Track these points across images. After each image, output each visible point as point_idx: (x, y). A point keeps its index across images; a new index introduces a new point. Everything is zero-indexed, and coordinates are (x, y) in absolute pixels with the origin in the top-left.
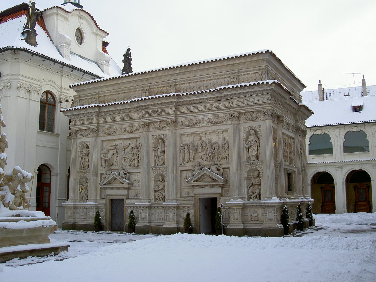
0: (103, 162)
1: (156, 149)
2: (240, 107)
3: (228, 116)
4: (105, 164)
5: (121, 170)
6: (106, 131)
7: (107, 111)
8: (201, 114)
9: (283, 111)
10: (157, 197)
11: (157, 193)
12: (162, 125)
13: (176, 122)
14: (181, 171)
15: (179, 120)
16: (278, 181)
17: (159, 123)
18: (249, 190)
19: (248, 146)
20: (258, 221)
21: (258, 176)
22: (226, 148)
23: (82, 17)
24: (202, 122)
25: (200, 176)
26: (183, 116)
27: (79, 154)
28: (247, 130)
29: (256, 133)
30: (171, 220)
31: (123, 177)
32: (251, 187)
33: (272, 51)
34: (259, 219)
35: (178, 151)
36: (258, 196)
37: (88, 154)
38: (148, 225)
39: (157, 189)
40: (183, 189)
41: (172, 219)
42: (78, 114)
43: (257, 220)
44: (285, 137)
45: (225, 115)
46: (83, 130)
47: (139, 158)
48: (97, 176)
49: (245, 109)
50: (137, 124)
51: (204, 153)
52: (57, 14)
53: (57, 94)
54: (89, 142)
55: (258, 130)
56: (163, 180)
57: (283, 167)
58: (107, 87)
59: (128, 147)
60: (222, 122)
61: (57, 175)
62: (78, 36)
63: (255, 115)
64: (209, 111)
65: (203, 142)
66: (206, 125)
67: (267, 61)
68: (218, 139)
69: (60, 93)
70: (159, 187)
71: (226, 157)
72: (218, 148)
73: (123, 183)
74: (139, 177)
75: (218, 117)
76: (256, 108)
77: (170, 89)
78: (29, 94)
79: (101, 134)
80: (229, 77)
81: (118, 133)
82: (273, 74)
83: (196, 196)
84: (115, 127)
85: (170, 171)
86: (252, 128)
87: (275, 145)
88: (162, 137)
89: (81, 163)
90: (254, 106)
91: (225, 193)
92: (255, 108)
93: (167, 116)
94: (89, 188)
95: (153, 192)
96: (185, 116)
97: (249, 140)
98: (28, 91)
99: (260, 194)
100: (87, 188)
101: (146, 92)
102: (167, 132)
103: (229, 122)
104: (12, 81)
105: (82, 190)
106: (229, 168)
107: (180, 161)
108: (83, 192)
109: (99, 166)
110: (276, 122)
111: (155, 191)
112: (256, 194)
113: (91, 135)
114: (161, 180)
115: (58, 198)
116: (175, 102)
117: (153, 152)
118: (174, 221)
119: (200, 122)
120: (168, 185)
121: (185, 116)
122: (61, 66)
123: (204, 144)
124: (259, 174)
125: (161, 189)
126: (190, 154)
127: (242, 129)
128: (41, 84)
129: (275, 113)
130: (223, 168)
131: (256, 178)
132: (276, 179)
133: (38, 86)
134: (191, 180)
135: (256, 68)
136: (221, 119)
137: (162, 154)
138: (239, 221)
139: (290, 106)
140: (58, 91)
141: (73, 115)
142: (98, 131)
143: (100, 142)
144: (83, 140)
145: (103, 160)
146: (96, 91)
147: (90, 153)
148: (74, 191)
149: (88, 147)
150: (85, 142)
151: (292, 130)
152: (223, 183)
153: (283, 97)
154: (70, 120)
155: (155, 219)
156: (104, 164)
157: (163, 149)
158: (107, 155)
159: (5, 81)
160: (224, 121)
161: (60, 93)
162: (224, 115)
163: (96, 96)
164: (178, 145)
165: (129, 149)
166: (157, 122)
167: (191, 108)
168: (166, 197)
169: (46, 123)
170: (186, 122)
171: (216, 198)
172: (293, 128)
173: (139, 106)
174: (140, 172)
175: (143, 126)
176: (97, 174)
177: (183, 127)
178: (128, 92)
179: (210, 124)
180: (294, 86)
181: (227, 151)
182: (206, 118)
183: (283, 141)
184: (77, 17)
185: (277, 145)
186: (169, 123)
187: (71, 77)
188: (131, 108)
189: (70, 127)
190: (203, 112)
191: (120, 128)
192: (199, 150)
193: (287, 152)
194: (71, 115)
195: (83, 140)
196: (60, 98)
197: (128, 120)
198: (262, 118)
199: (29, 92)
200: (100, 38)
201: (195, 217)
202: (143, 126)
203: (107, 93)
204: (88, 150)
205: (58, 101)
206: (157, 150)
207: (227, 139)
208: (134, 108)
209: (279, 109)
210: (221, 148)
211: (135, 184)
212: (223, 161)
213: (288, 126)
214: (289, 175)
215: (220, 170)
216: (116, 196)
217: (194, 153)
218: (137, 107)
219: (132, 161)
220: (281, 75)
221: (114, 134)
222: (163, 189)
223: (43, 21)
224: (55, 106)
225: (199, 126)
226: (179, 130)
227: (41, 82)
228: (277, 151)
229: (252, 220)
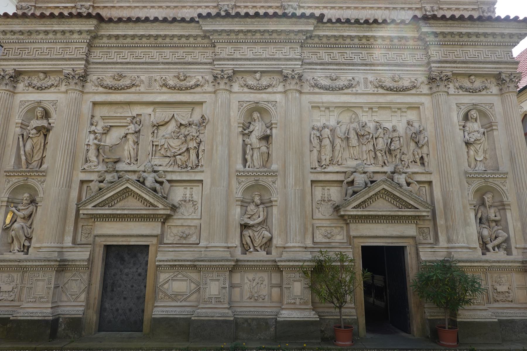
4: (97, 157)
5: (150, 172)
8: (359, 70)
11: (248, 233)
12: (265, 81)
26: (316, 69)
40: (318, 225)
41: (301, 299)
47: (202, 147)
48: (70, 187)
49: (464, 67)
59: (167, 123)
63: (478, 83)
66: (371, 92)
68: (398, 122)
70: (254, 217)
79: (90, 87)
81: (142, 89)
88: (263, 105)
89: (22, 152)
92: (485, 68)
93: (284, 63)
95: (239, 230)
96: (321, 69)
111: (245, 226)
113: (63, 88)
117: (241, 136)
121: (321, 69)
125: (259, 224)
141: (13, 32)
142: (83, 78)
144: (35, 97)
149: (46, 115)
150: (40, 102)
156: (93, 158)
166: (256, 72)
195: (35, 97)
211: (182, 210)
216: (124, 239)
219: (180, 155)
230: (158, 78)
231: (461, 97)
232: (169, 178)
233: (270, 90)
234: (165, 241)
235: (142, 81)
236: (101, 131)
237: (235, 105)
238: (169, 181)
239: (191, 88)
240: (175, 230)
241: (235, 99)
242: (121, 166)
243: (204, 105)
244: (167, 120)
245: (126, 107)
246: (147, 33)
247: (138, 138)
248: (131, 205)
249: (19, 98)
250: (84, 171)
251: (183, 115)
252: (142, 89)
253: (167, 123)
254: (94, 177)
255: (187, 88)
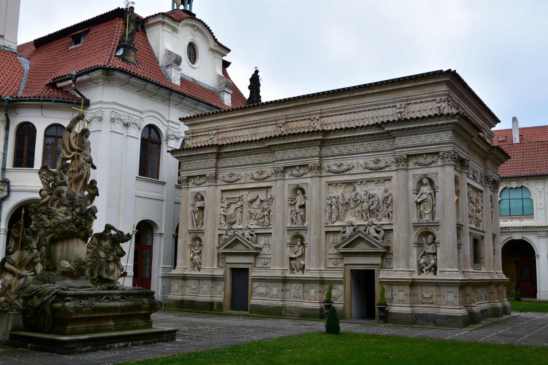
0: (223, 218)
1: (293, 203)
2: (409, 147)
3: (393, 160)
4: (225, 221)
5: (246, 230)
6: (227, 179)
7: (229, 152)
9: (468, 154)
10: (293, 266)
11: (292, 262)
12: (302, 171)
13: (320, 168)
14: (327, 232)
15: (325, 165)
16: (461, 250)
17: (297, 168)
18: (420, 261)
19: (420, 200)
20: (432, 303)
21: (433, 242)
22: (389, 202)
23: (196, 28)
24: (356, 168)
25: (352, 239)
27: (190, 209)
28: (418, 178)
29: (431, 182)
30: (312, 299)
31: (248, 239)
32: (424, 257)
33: (455, 71)
34: (434, 301)
35: (324, 206)
36: (433, 269)
37: (202, 209)
38: (280, 303)
39: (294, 256)
42: (191, 156)
43: (431, 302)
44: (471, 190)
45: (387, 159)
46: (195, 176)
47: (271, 214)
48: (214, 238)
50: (268, 170)
51: (359, 208)
52: (163, 23)
53: (163, 130)
54: (205, 192)
55: (434, 179)
56: (302, 244)
57: (466, 230)
58: (229, 120)
59: (255, 200)
60: (383, 168)
61: (161, 235)
62: (190, 54)
64: (365, 153)
65: (357, 194)
66: (361, 172)
67: (448, 83)
69: (167, 128)
71: (389, 215)
72: (378, 203)
73: (248, 248)
74: (271, 240)
75: (378, 161)
76: (433, 149)
77: (313, 122)
78: (125, 128)
79: (219, 182)
80: (394, 106)
81: (242, 181)
82: (456, 103)
83: (347, 267)
84: (238, 173)
85: (312, 233)
86: (425, 176)
87: (457, 201)
90: (428, 145)
91: (387, 265)
94: (203, 253)
95: (289, 260)
97: (421, 192)
98: (124, 124)
99: (435, 266)
100: (200, 252)
101: (281, 127)
102: (308, 181)
103: (394, 167)
104: (103, 110)
105: (194, 255)
106: (392, 230)
107: (325, 218)
108: (195, 257)
109: (218, 224)
110: (459, 169)
111: (291, 259)
112: (429, 266)
113: (208, 184)
114: (299, 244)
115: (161, 266)
116: (320, 140)
118: (316, 300)
119: (353, 167)
120: (309, 251)
122: (168, 92)
123: (358, 197)
124: (434, 238)
125: (300, 257)
126: (339, 210)
127: (411, 177)
128: (143, 116)
129: (458, 156)
130: (384, 230)
131: (430, 244)
132: (459, 246)
133: (138, 118)
134: (339, 245)
135: (432, 94)
136: (382, 164)
137: (302, 210)
138: (406, 303)
139: (478, 146)
140: (165, 126)
141: (184, 157)
142: (216, 178)
143: (219, 193)
145: (222, 216)
146: (215, 125)
147: (206, 207)
148: (184, 257)
149: (202, 199)
151: (480, 180)
152: (384, 251)
153: (469, 134)
154: (180, 163)
155: (290, 296)
156: (224, 222)
157: (303, 203)
158: (227, 210)
159: (94, 111)
160: (386, 166)
161: (167, 128)
162: (386, 159)
163: (214, 132)
164: (323, 197)
165: (258, 202)
166: (296, 166)
167: (342, 149)
168: (307, 267)
169: (148, 167)
170: (334, 168)
171: (374, 270)
172: (482, 177)
173: (272, 146)
174: (271, 233)
175: (276, 173)
176: (214, 235)
177: (330, 174)
178: (256, 127)
179: (367, 171)
180: (484, 119)
181: (390, 207)
182: (361, 161)
183: (468, 195)
184: (189, 28)
185: (460, 201)
186: (311, 169)
187: (181, 107)
188: (261, 148)
189: (179, 172)
190: (358, 154)
191: (246, 174)
192: (352, 205)
193: (473, 210)
194: (181, 157)
196: (167, 135)
197: (257, 164)
198: (440, 162)
199: (126, 125)
200: (220, 57)
201: (345, 295)
202: (276, 173)
203: (229, 128)
204: (202, 202)
205: (164, 137)
206: (295, 204)
207: (390, 191)
208: (265, 148)
209: (464, 151)
210: (381, 203)
211: (264, 249)
212: (385, 221)
213: (475, 175)
214: (476, 243)
215: (381, 233)
217: (345, 208)
218: (269, 147)
219: (261, 218)
220: (466, 104)
221: (238, 182)
222: (302, 256)
223: (145, 33)
224: (159, 144)
225: (351, 173)
226: (325, 178)
227: (142, 113)
228: (460, 208)
229: (424, 302)
230: (249, 174)
231: (417, 170)
232: (256, 232)
233: (305, 176)
234: (257, 266)
235: (242, 176)
236: (226, 206)
237: (286, 187)
238: (257, 234)
239: (265, 179)
240: (261, 260)
241: (287, 183)
242: (234, 226)
243: (272, 188)
244: (255, 198)
245: (237, 192)
246: (241, 149)
247: (242, 209)
248: (239, 248)
249: (191, 190)
250: (219, 229)
251: (262, 195)
252: (242, 181)
253: (255, 200)
254: (223, 232)
255: (263, 179)
